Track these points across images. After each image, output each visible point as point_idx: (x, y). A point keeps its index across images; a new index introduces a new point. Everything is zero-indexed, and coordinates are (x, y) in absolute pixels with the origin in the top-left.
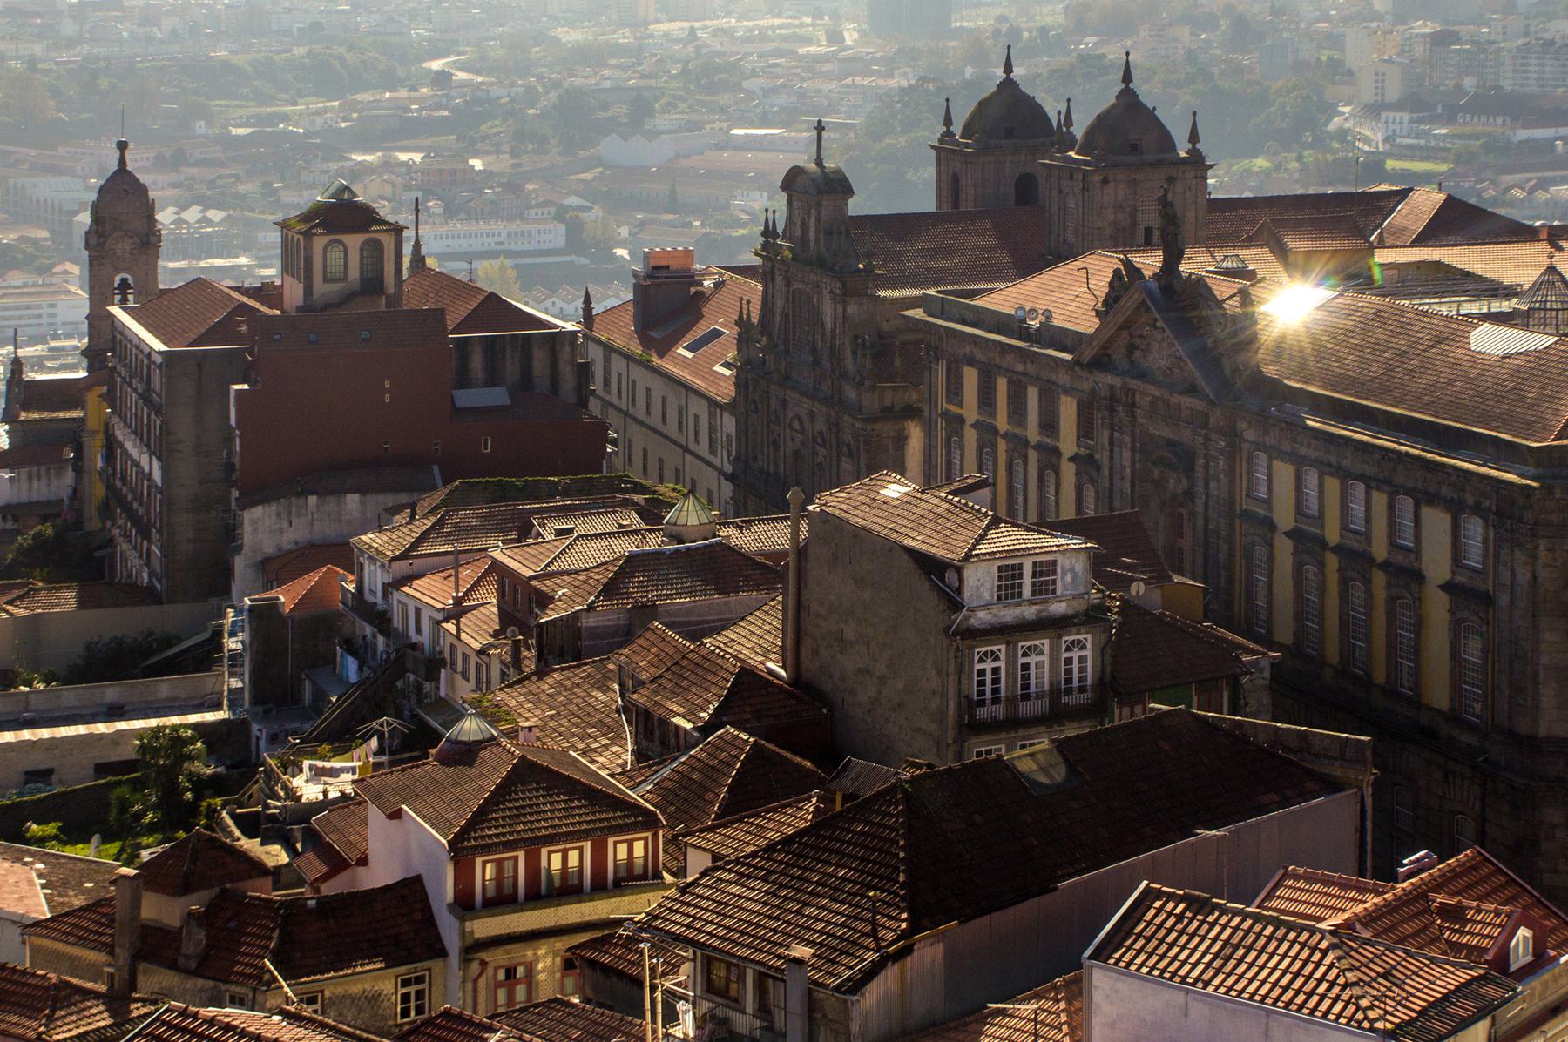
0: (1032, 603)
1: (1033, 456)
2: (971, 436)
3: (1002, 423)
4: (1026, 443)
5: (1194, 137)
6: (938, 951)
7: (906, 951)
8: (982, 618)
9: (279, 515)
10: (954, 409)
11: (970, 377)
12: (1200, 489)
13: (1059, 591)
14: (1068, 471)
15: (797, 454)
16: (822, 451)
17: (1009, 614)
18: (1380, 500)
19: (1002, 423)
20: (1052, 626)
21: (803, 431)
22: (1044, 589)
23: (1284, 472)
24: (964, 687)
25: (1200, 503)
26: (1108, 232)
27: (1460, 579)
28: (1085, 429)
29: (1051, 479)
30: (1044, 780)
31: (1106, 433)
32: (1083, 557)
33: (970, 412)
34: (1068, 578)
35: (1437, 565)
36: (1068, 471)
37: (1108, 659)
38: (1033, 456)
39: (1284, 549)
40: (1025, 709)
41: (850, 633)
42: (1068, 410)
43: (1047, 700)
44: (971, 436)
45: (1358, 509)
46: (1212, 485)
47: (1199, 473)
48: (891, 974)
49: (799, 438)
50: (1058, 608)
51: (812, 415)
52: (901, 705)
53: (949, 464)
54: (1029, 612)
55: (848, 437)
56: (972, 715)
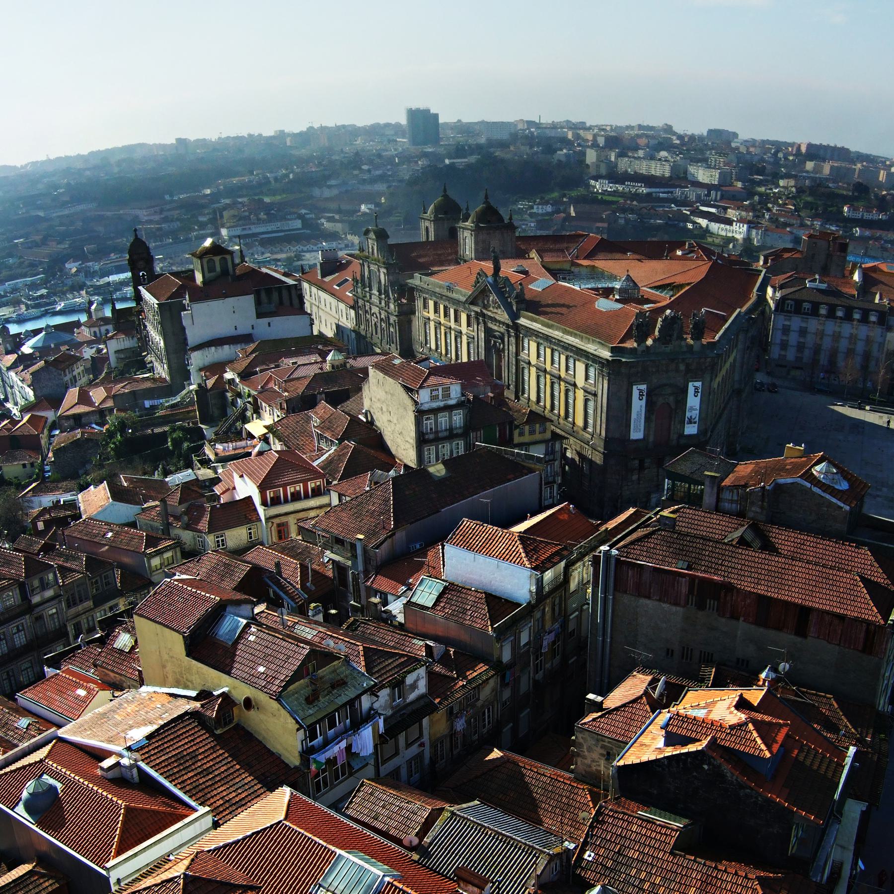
0: (442, 401)
1: (453, 332)
2: (432, 324)
3: (442, 320)
4: (450, 328)
5: (511, 219)
6: (404, 533)
7: (394, 534)
8: (426, 407)
9: (203, 355)
10: (426, 314)
11: (431, 304)
12: (506, 347)
13: (452, 396)
14: (464, 338)
15: (375, 324)
16: (384, 325)
17: (435, 405)
18: (563, 358)
19: (442, 320)
20: (449, 408)
21: (377, 318)
22: (447, 395)
23: (533, 345)
24: (421, 428)
25: (506, 352)
26: (480, 250)
27: (586, 386)
28: (469, 324)
29: (459, 340)
30: (439, 475)
31: (476, 327)
32: (459, 385)
33: (432, 315)
34: (454, 392)
35: (580, 381)
36: (464, 338)
37: (468, 418)
38: (453, 332)
39: (533, 370)
40: (441, 435)
41: (384, 409)
42: (464, 317)
43: (448, 432)
44: (432, 324)
45: (556, 358)
46: (510, 347)
47: (506, 343)
48: (389, 540)
49: (376, 320)
50: (452, 402)
51: (380, 313)
52: (401, 433)
53: (426, 332)
54: (441, 404)
55: (392, 321)
56: (424, 438)
